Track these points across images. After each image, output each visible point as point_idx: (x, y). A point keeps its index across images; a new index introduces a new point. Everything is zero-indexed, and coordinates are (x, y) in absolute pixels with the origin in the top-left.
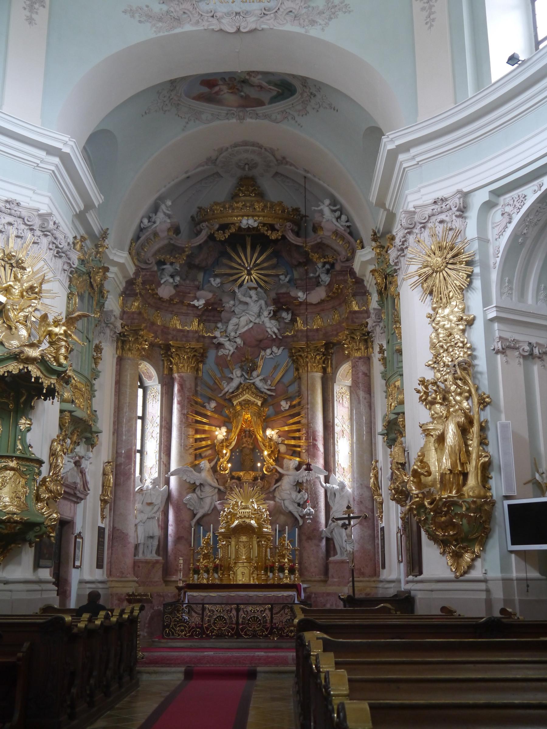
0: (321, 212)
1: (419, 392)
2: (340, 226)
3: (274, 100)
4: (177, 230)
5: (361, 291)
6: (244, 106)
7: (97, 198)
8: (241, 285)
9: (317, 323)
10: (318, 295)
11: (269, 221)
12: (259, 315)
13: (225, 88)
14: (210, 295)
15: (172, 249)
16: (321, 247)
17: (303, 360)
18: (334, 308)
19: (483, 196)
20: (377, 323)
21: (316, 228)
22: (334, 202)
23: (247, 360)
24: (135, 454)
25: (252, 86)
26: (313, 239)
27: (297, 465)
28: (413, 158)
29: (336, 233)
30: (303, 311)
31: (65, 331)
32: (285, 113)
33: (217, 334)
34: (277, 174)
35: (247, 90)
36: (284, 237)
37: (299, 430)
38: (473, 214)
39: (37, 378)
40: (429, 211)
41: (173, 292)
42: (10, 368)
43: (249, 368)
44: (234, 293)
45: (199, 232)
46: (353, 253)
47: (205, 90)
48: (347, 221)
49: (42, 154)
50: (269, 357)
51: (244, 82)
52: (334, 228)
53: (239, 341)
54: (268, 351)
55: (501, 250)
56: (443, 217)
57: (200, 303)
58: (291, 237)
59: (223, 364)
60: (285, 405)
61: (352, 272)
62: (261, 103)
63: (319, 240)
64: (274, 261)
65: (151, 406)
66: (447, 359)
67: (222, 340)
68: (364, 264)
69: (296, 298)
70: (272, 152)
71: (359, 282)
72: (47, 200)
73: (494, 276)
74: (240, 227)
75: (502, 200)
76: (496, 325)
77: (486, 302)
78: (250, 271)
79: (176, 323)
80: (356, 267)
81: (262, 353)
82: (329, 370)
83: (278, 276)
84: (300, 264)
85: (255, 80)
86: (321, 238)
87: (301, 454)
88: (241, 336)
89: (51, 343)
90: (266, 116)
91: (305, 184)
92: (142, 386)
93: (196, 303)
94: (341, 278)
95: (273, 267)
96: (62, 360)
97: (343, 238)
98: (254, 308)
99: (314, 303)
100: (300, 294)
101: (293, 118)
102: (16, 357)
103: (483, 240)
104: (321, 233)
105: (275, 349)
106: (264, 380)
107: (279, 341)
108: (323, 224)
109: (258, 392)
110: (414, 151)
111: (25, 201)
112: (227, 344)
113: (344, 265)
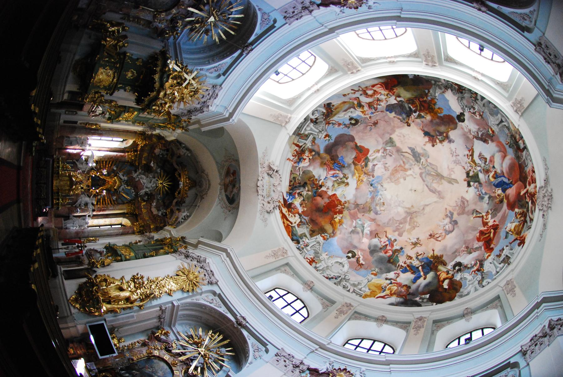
0: (184, 212)
1: (137, 275)
2: (180, 219)
3: (227, 196)
4: (179, 157)
5: (158, 229)
6: (224, 184)
7: (203, 129)
8: (157, 180)
9: (144, 211)
10: (155, 211)
11: (182, 193)
12: (147, 187)
13: (232, 178)
14: (154, 168)
15: (173, 154)
16: (172, 212)
18: (150, 217)
19: (218, 291)
21: (179, 210)
22: (188, 217)
23: (131, 182)
25: (233, 188)
26: (175, 209)
29: (177, 218)
31: (165, 110)
33: (140, 171)
35: (231, 187)
36: (175, 198)
38: (210, 288)
39: (149, 95)
40: (208, 269)
41: (157, 154)
42: (157, 83)
43: (127, 183)
44: (155, 178)
45: (178, 165)
46: (171, 225)
47: (232, 171)
49: (231, 111)
51: (234, 186)
53: (137, 179)
54: (133, 191)
55: (199, 302)
56: (207, 275)
57: (152, 164)
58: (175, 201)
59: (128, 173)
60: (114, 198)
61: (165, 226)
62: (226, 191)
64: (165, 193)
65: (116, 143)
66: (153, 287)
67: (138, 173)
68: (170, 232)
69: (153, 202)
70: (206, 194)
71: (161, 228)
72: (213, 110)
73: (189, 300)
74: (179, 181)
75: (217, 298)
76: (170, 305)
77: (179, 300)
78: (161, 183)
79: (145, 155)
80: (167, 228)
83: (160, 194)
84: (164, 203)
85: (235, 190)
88: (139, 180)
89: (161, 104)
90: (220, 193)
91: (193, 206)
92: (124, 140)
93: (152, 163)
95: (163, 192)
96: (154, 107)
97: (176, 220)
98: (149, 185)
100: (155, 204)
102: (162, 86)
103: (201, 294)
106: (123, 189)
107: (137, 195)
109: (119, 187)
110: (228, 259)
111: (216, 101)
112: (136, 175)
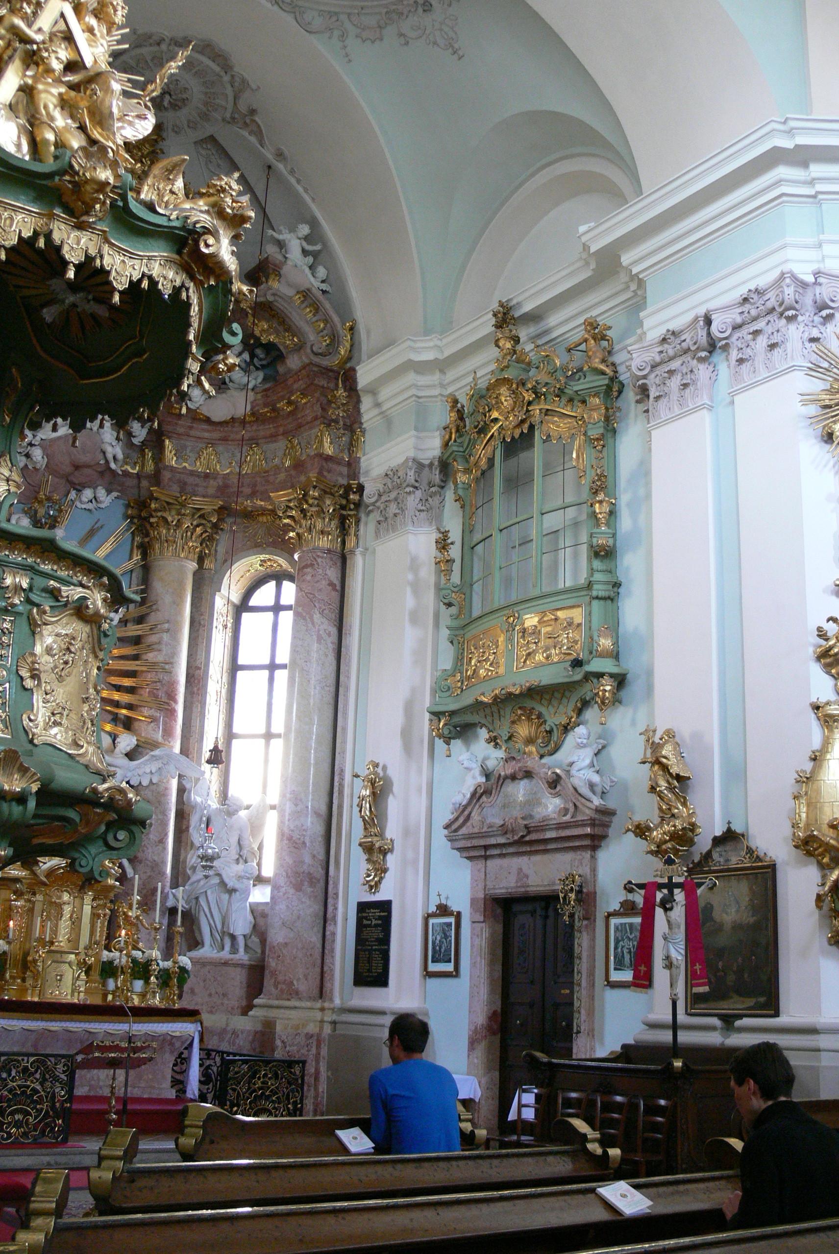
17: (169, 529)
20: (411, 489)
24: (293, 661)
27: (133, 746)
28: (812, 182)
29: (306, 294)
30: (181, 430)
32: (334, 19)
34: (212, 139)
37: (132, 674)
48: (323, 282)
50: (84, 506)
52: (308, 286)
54: (88, 494)
63: (270, 298)
81: (73, 495)
82: (207, 564)
86: (274, 295)
87: (136, 725)
94: (323, 382)
99: (215, 418)
101: (343, 37)
104: (274, 284)
105: (101, 492)
108: (285, 270)
110: (817, 170)
113: (316, 360)
